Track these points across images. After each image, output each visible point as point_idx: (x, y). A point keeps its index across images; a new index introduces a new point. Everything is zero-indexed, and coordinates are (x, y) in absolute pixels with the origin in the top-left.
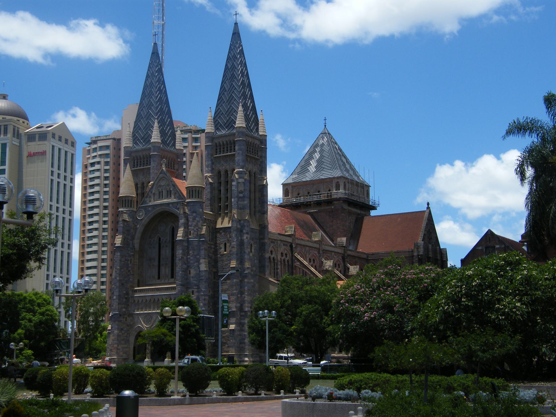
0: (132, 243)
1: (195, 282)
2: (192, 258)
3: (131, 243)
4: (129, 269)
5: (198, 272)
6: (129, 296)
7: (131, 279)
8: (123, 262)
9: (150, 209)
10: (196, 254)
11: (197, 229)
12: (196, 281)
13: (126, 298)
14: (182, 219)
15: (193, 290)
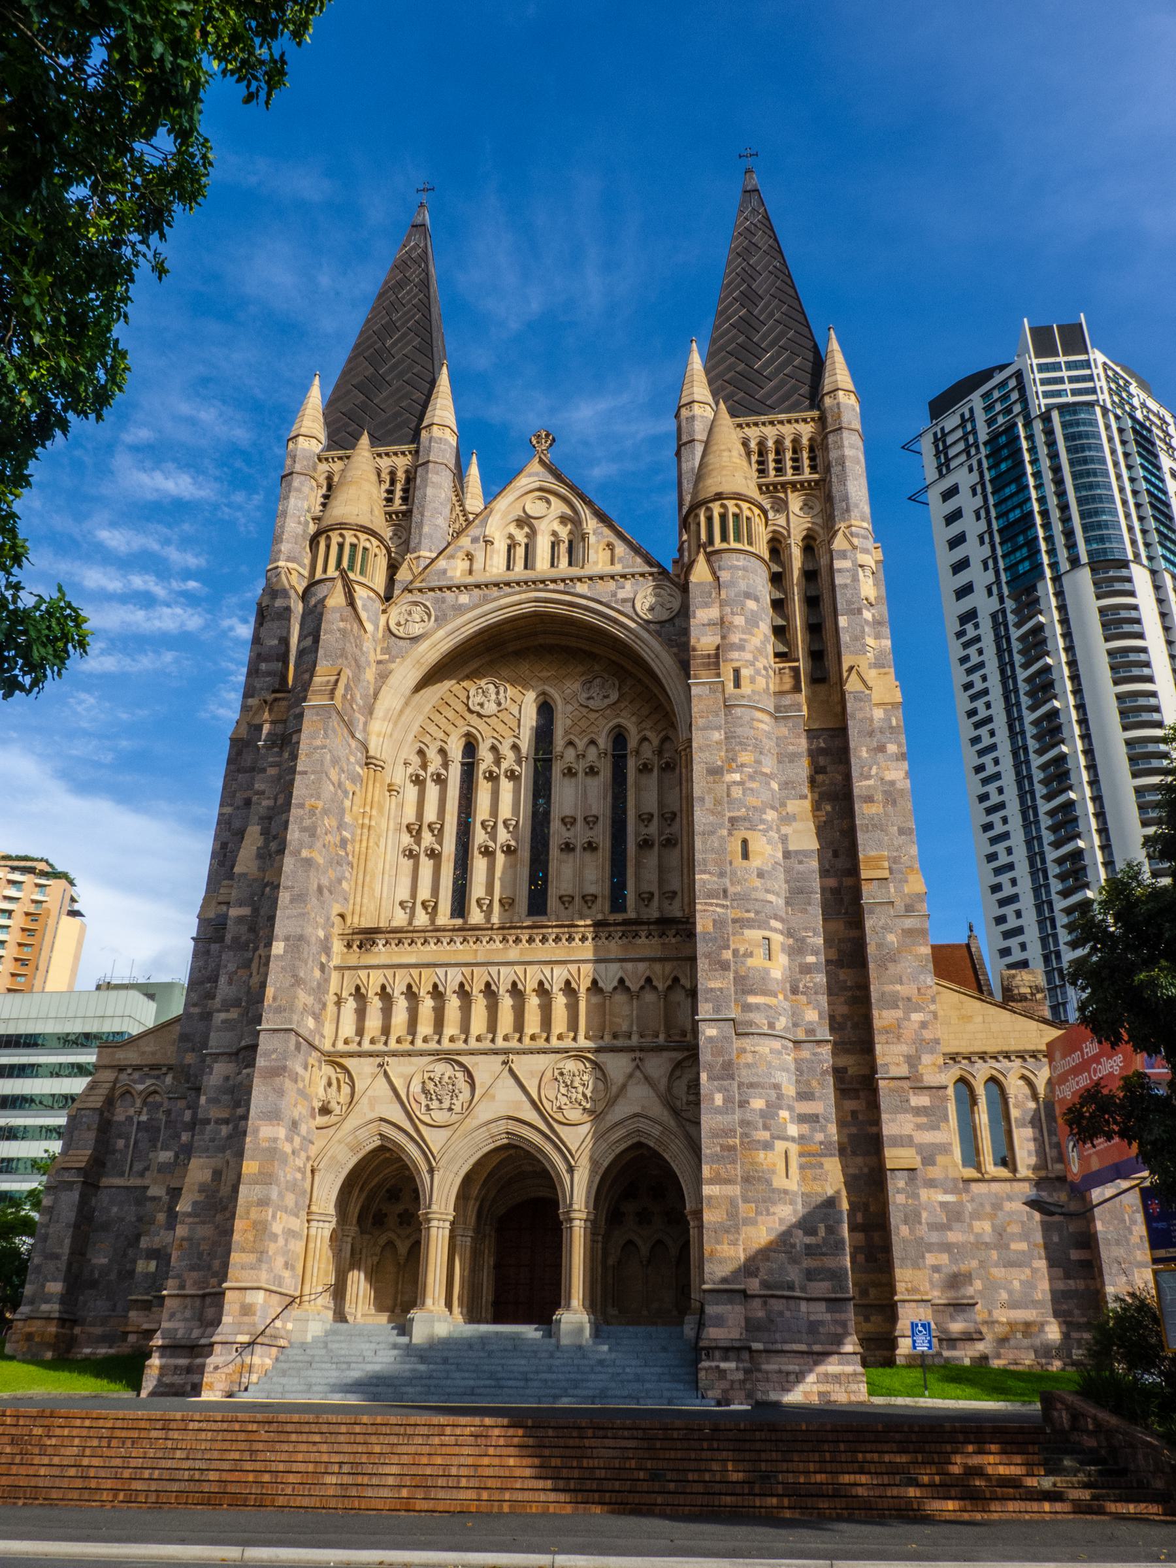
0: (365, 724)
1: (771, 897)
2: (754, 785)
3: (361, 726)
4: (345, 833)
5: (780, 855)
6: (332, 964)
7: (345, 885)
8: (331, 788)
9: (464, 599)
10: (767, 770)
11: (765, 668)
12: (778, 894)
13: (323, 968)
14: (707, 605)
15: (767, 934)
